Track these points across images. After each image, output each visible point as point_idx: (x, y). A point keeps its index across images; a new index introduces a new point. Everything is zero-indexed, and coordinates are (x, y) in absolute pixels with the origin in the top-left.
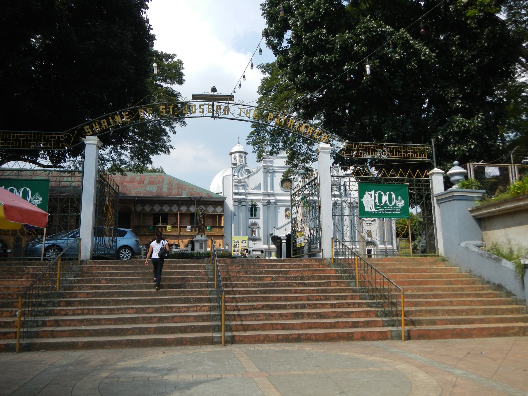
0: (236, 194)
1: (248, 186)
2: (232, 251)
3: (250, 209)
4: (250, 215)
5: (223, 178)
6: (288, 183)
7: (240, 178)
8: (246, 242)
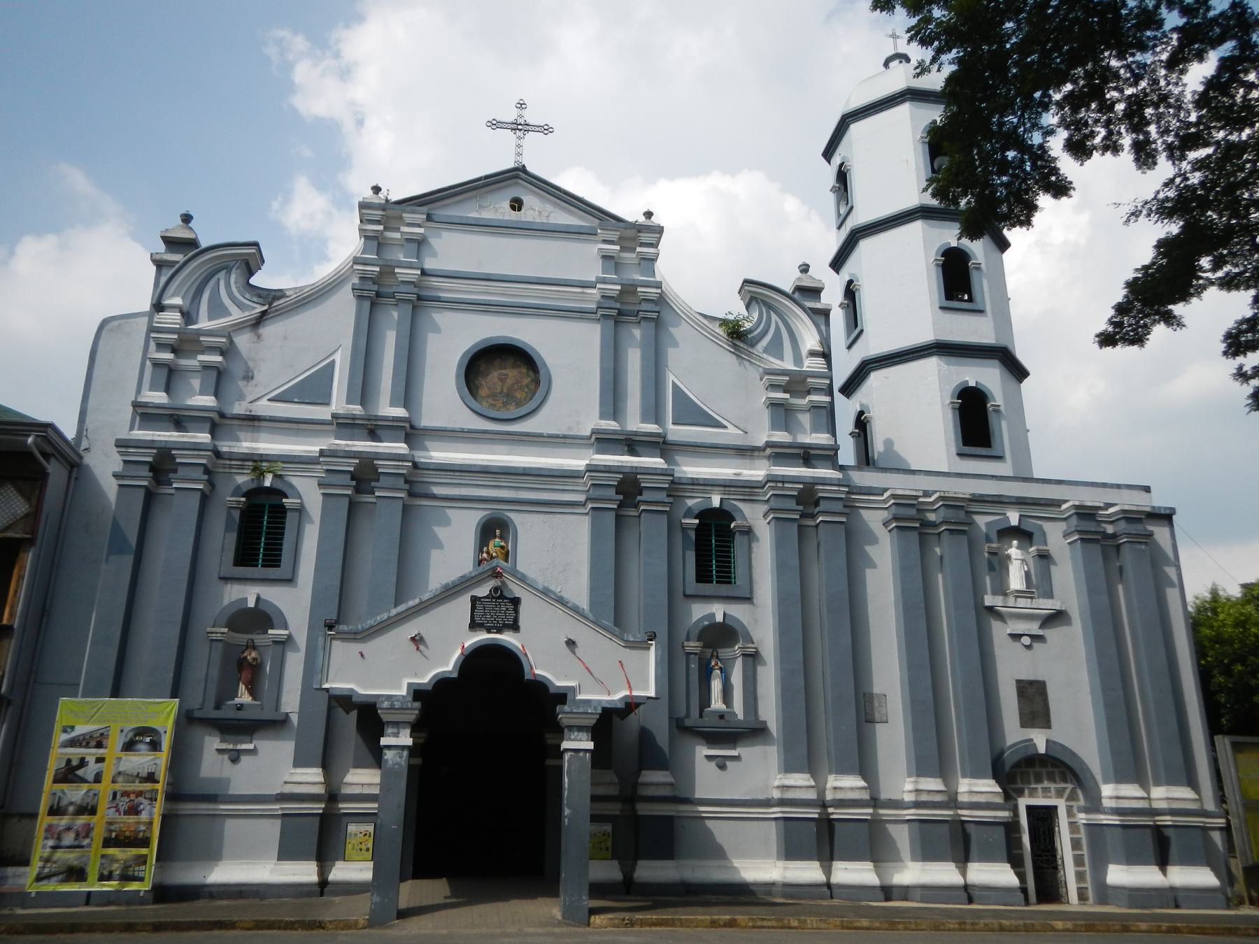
0: (146, 415)
1: (249, 377)
2: (43, 807)
3: (236, 515)
4: (230, 555)
6: (513, 374)
7: (204, 324)
8: (155, 746)
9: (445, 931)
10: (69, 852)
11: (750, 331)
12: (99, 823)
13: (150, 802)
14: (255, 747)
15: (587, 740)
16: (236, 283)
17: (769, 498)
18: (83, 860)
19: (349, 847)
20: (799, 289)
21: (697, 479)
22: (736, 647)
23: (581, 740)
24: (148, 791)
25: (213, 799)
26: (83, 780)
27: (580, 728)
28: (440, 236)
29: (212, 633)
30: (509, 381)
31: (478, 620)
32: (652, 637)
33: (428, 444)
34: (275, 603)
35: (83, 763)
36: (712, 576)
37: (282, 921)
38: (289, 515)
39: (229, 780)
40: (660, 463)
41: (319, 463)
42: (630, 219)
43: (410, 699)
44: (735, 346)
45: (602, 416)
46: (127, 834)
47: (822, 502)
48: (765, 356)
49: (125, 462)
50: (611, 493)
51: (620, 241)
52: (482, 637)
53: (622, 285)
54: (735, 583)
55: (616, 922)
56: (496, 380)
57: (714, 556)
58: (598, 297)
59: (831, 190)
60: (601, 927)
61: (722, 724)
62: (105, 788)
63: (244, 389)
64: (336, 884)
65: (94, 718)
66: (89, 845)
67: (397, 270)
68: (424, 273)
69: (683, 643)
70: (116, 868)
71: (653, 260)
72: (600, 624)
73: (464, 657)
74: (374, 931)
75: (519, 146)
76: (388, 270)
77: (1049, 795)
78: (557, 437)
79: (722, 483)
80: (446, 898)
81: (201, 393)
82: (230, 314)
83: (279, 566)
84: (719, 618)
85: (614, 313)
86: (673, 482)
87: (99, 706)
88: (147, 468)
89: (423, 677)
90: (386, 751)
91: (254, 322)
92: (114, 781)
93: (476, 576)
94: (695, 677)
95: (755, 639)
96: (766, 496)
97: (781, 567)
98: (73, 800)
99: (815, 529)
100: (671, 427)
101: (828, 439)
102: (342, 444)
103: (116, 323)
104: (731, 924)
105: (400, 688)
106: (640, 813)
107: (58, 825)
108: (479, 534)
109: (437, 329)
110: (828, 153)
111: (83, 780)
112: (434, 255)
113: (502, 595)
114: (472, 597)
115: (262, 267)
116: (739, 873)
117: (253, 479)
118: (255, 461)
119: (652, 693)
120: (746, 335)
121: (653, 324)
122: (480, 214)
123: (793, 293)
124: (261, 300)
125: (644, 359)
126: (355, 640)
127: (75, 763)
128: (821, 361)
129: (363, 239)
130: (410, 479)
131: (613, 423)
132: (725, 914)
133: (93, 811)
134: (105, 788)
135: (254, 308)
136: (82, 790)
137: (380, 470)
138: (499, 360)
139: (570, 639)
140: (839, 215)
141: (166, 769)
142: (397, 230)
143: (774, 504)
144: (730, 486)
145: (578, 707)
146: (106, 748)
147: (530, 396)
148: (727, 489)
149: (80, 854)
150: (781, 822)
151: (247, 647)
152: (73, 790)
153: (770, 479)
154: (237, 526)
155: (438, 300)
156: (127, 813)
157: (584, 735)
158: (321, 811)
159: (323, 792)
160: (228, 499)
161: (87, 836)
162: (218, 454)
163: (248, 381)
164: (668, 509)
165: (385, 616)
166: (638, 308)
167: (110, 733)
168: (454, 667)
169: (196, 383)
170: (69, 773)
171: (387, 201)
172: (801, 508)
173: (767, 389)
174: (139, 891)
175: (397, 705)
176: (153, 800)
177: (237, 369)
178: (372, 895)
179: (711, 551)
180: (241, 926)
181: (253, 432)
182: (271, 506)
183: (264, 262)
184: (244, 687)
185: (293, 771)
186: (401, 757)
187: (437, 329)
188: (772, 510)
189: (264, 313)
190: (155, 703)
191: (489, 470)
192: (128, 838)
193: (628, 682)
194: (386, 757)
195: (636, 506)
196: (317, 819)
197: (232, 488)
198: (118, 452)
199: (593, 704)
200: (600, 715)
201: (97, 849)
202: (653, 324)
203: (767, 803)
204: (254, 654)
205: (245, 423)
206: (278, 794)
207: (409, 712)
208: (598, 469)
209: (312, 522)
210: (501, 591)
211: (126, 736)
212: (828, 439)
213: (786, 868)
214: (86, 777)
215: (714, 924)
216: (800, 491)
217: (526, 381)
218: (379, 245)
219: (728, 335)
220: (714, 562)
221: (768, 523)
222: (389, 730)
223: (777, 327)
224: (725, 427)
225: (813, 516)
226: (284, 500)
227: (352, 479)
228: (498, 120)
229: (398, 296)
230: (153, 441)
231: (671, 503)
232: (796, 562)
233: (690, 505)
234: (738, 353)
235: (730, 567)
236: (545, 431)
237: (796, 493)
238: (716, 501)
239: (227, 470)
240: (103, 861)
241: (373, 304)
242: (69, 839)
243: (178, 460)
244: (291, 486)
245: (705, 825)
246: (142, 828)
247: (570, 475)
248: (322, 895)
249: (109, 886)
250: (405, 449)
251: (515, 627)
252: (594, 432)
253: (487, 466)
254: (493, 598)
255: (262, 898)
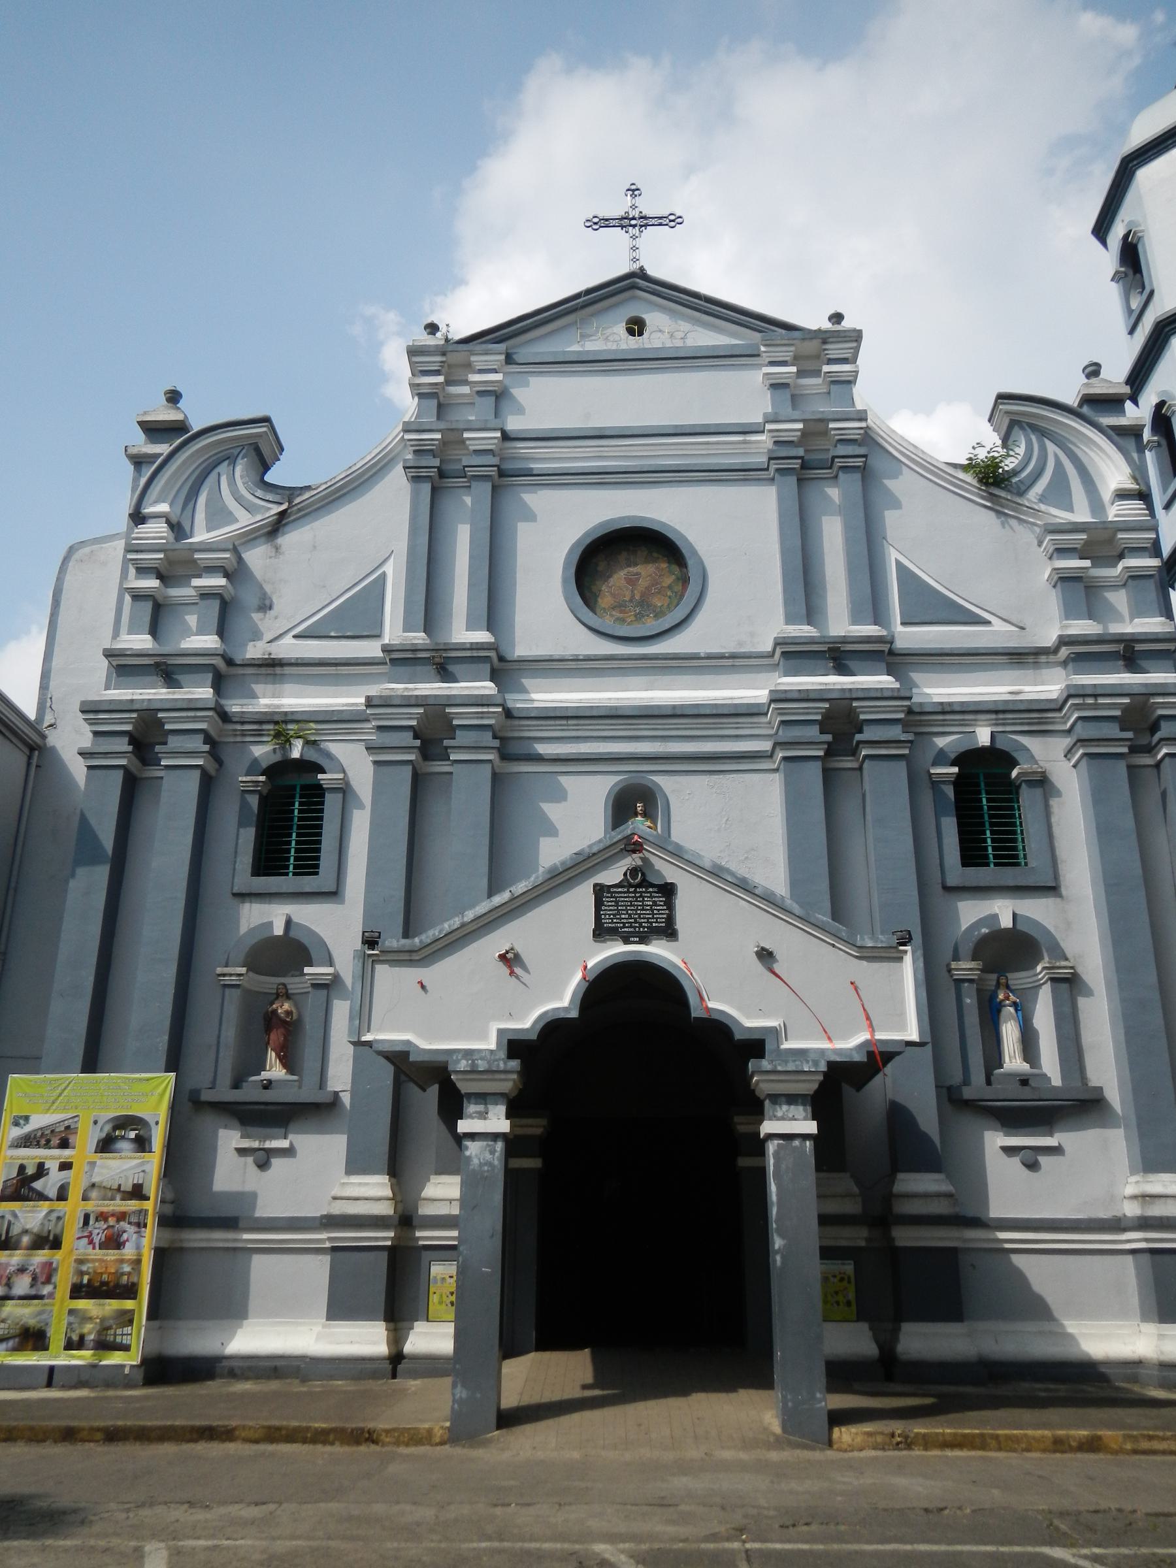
1: (265, 606)
3: (254, 801)
4: (246, 860)
5: (66, 560)
7: (200, 536)
8: (142, 1144)
9: (576, 1455)
10: (23, 1305)
11: (1015, 472)
12: (65, 1261)
13: (136, 1229)
14: (291, 1144)
15: (805, 1119)
16: (242, 477)
17: (1073, 726)
18: (44, 1317)
19: (434, 1299)
20: (1090, 400)
21: (950, 704)
22: (1039, 968)
23: (794, 1119)
24: (134, 1212)
25: (230, 1223)
26: (42, 1197)
27: (792, 1099)
28: (527, 385)
29: (224, 975)
30: (643, 583)
31: (607, 922)
32: (905, 940)
33: (527, 682)
34: (313, 927)
35: (41, 1171)
36: (987, 857)
37: (308, 1429)
38: (329, 797)
39: (253, 1196)
40: (888, 682)
41: (367, 720)
42: (813, 325)
43: (503, 1054)
44: (992, 497)
45: (790, 619)
46: (105, 1277)
47: (1163, 724)
48: (1043, 507)
49: (96, 734)
50: (813, 732)
51: (796, 360)
52: (616, 950)
53: (803, 421)
54: (1026, 864)
55: (879, 1439)
56: (623, 582)
57: (987, 824)
58: (770, 445)
59: (1112, 280)
60: (851, 1448)
61: (1026, 1092)
62: (73, 1209)
63: (259, 623)
64: (416, 1358)
65: (56, 1105)
66: (51, 1295)
67: (466, 435)
68: (506, 437)
69: (948, 965)
70: (90, 1330)
71: (849, 382)
72: (812, 920)
73: (587, 984)
74: (458, 1451)
75: (634, 248)
76: (453, 440)
78: (721, 657)
79: (992, 707)
80: (585, 1387)
81: (201, 631)
82: (237, 521)
83: (317, 873)
84: (1006, 922)
85: (796, 464)
86: (910, 711)
87: (64, 1086)
88: (126, 740)
89: (522, 1018)
90: (468, 1143)
91: (270, 529)
92: (85, 1198)
93: (600, 852)
94: (972, 1019)
95: (1069, 955)
96: (1065, 723)
97: (1104, 832)
98: (28, 1227)
99: (1155, 771)
100: (899, 629)
101: (1163, 624)
102: (399, 688)
103: (86, 550)
104: (1092, 1445)
105: (484, 1037)
106: (900, 1243)
107: (8, 1265)
108: (610, 812)
109: (530, 517)
110: (1101, 230)
111: (42, 1197)
112: (520, 410)
113: (644, 880)
114: (595, 885)
115: (281, 457)
116: (1078, 1344)
117: (274, 750)
118: (276, 723)
119: (913, 1035)
120: (1008, 479)
121: (858, 476)
122: (583, 346)
123: (1081, 405)
124: (277, 498)
125: (848, 528)
126: (411, 963)
127: (30, 1171)
128: (1139, 504)
129: (416, 399)
130: (500, 734)
131: (807, 628)
132: (1078, 1428)
133: (56, 1244)
134: (73, 1209)
135: (270, 509)
136: (40, 1212)
137: (455, 722)
138: (624, 555)
139: (763, 949)
140: (1130, 311)
141: (159, 1179)
142: (466, 382)
143: (1082, 731)
144: (1004, 712)
145: (786, 1062)
146: (74, 1148)
147: (676, 601)
148: (1001, 716)
149: (39, 1308)
150: (1146, 1258)
151: (278, 996)
152: (29, 1212)
153: (1072, 692)
154: (255, 819)
155: (529, 473)
156: (104, 1246)
157: (799, 1110)
158: (389, 1243)
159: (391, 1212)
160: (240, 779)
161: (48, 1280)
162: (225, 717)
163: (265, 612)
164: (906, 751)
165: (456, 922)
166: (833, 453)
167: (79, 1125)
168: (572, 1001)
169: (192, 620)
170: (23, 1186)
171: (447, 340)
172: (1129, 735)
173: (1050, 558)
174: (123, 1366)
175: (482, 1065)
176: (141, 1225)
177: (249, 598)
178: (454, 1386)
179: (982, 816)
180: (243, 1435)
181: (274, 683)
182: (303, 787)
183: (282, 450)
184: (274, 1054)
185: (345, 1180)
186: (493, 1152)
187: (530, 517)
188: (1081, 741)
189: (282, 514)
190: (140, 1080)
191: (620, 713)
192: (103, 1284)
193: (868, 1018)
194: (467, 1153)
195: (854, 752)
196: (384, 1255)
197: (246, 764)
198: (85, 720)
199: (812, 1056)
200: (825, 1074)
201: (62, 1302)
202: (858, 476)
203: (1117, 1225)
204: (286, 1006)
205: (263, 670)
206: (323, 1217)
207: (503, 1076)
208: (789, 696)
209: (361, 806)
210: (643, 874)
211: (101, 1129)
212: (1163, 624)
213: (1161, 1337)
214: (46, 1193)
215: (1059, 1445)
216: (1126, 709)
217: (668, 580)
218: (440, 406)
219: (980, 481)
220: (988, 832)
221: (1074, 766)
222: (471, 1108)
223: (1059, 464)
224: (988, 623)
225: (1150, 749)
226: (320, 776)
227: (416, 737)
228: (601, 215)
229: (471, 472)
230: (132, 701)
231: (911, 742)
232: (1129, 822)
233: (941, 746)
234: (997, 507)
235: (1015, 840)
236: (702, 650)
237: (1118, 713)
238: (983, 736)
239: (239, 739)
240: (72, 1319)
241: (434, 490)
242: (22, 1285)
243: (167, 727)
244: (329, 755)
245: (1010, 1258)
246: (127, 1268)
247: (750, 712)
248: (394, 1376)
249: (80, 1358)
250: (490, 688)
251: (669, 931)
252: (778, 643)
253: (616, 708)
254: (631, 886)
255: (304, 1380)
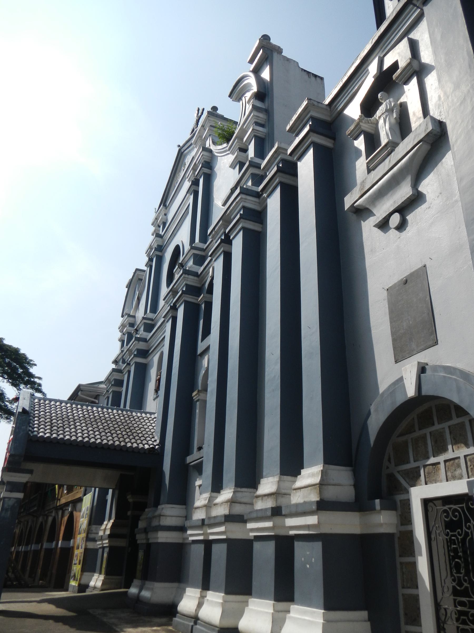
77: (458, 472)
